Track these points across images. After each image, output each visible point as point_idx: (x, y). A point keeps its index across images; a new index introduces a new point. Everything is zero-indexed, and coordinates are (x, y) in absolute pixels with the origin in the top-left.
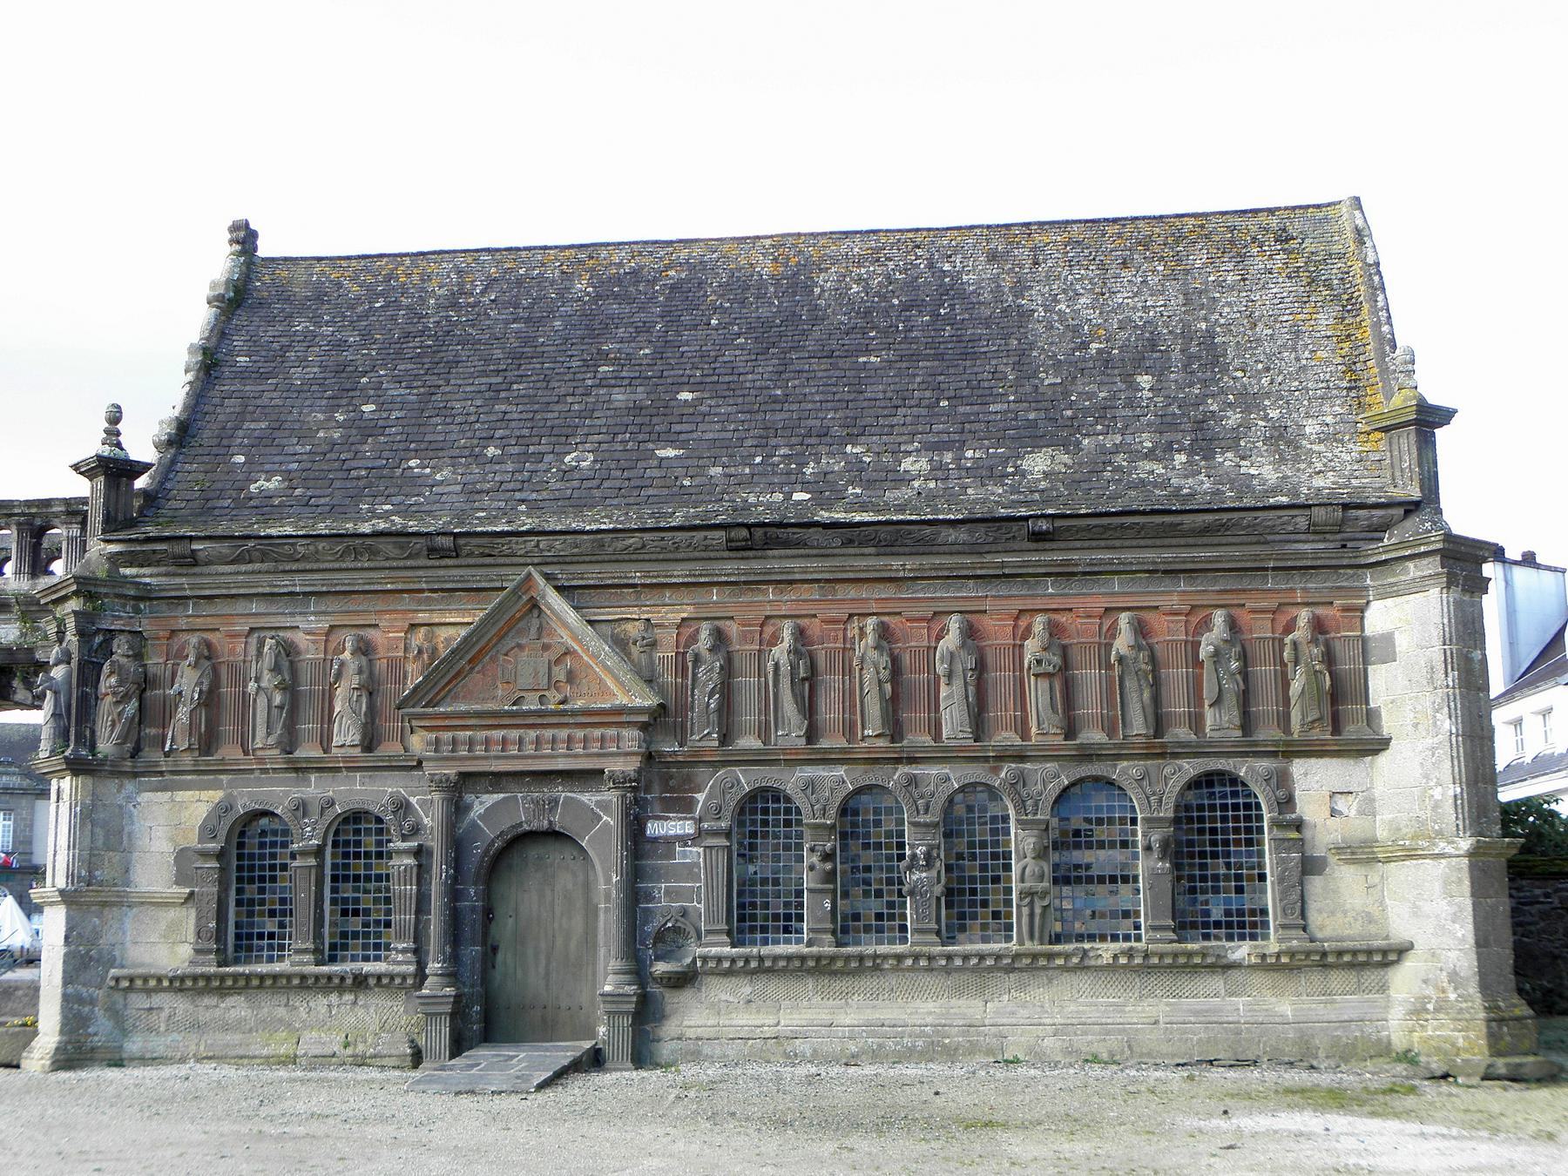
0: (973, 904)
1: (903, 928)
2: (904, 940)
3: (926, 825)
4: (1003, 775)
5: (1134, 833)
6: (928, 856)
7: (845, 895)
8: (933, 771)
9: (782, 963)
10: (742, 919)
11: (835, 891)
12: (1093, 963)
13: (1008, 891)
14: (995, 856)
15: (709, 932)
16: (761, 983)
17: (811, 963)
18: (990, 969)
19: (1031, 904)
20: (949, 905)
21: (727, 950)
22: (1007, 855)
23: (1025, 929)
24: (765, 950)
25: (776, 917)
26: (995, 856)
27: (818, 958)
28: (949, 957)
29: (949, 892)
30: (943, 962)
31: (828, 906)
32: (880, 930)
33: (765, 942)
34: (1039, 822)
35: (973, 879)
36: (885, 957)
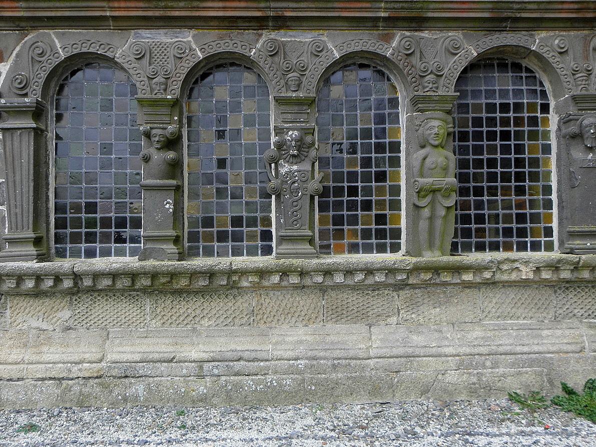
0: (352, 206)
1: (266, 236)
2: (267, 251)
3: (299, 102)
5: (546, 121)
6: (301, 145)
7: (194, 195)
8: (305, 37)
9: (106, 282)
10: (61, 224)
11: (178, 189)
12: (505, 277)
13: (396, 190)
14: (380, 148)
15: (12, 242)
16: (84, 304)
17: (146, 282)
18: (377, 287)
19: (432, 203)
20: (323, 207)
21: (34, 265)
22: (395, 147)
24: (82, 264)
25: (106, 223)
26: (380, 148)
27: (154, 275)
28: (328, 272)
29: (325, 193)
30: (320, 279)
31: (169, 207)
32: (237, 237)
33: (90, 254)
34: (443, 99)
35: (352, 176)
36: (243, 273)
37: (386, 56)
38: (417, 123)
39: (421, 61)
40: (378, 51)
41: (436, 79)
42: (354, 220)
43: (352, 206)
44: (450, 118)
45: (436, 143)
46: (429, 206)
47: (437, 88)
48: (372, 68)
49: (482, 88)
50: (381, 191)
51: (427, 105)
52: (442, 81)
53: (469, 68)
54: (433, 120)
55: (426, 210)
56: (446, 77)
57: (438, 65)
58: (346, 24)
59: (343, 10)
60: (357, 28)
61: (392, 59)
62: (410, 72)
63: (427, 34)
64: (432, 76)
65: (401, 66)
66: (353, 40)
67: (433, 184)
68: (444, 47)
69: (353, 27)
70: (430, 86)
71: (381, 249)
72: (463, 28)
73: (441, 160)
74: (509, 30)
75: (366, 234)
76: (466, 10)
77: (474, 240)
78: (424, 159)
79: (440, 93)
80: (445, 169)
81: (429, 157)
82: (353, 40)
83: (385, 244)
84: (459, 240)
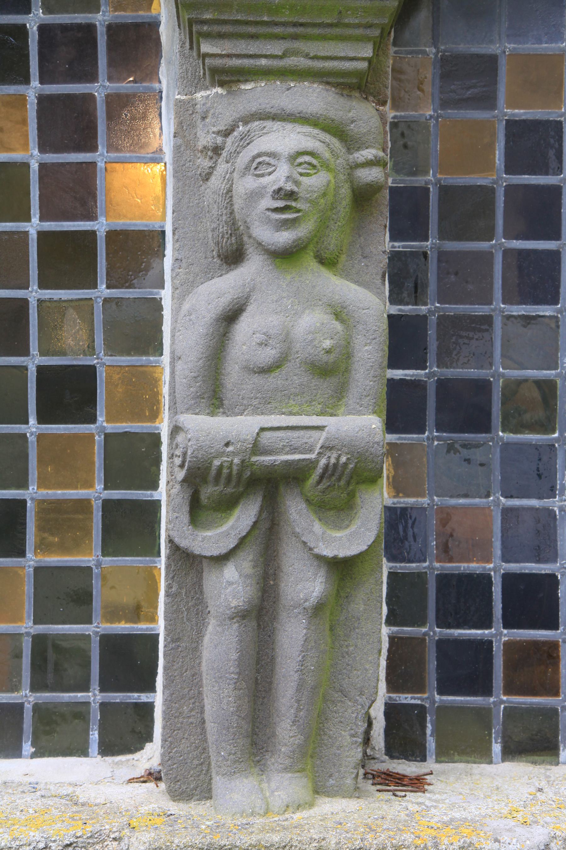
19: (267, 539)
23: (219, 699)
44: (364, 116)
45: (284, 238)
51: (242, 47)
54: (277, 125)
55: (230, 572)
67: (257, 448)
73: (312, 326)
77: (500, 700)
78: (231, 316)
80: (331, 372)
81: (251, 309)
83: (80, 713)
84: (432, 698)
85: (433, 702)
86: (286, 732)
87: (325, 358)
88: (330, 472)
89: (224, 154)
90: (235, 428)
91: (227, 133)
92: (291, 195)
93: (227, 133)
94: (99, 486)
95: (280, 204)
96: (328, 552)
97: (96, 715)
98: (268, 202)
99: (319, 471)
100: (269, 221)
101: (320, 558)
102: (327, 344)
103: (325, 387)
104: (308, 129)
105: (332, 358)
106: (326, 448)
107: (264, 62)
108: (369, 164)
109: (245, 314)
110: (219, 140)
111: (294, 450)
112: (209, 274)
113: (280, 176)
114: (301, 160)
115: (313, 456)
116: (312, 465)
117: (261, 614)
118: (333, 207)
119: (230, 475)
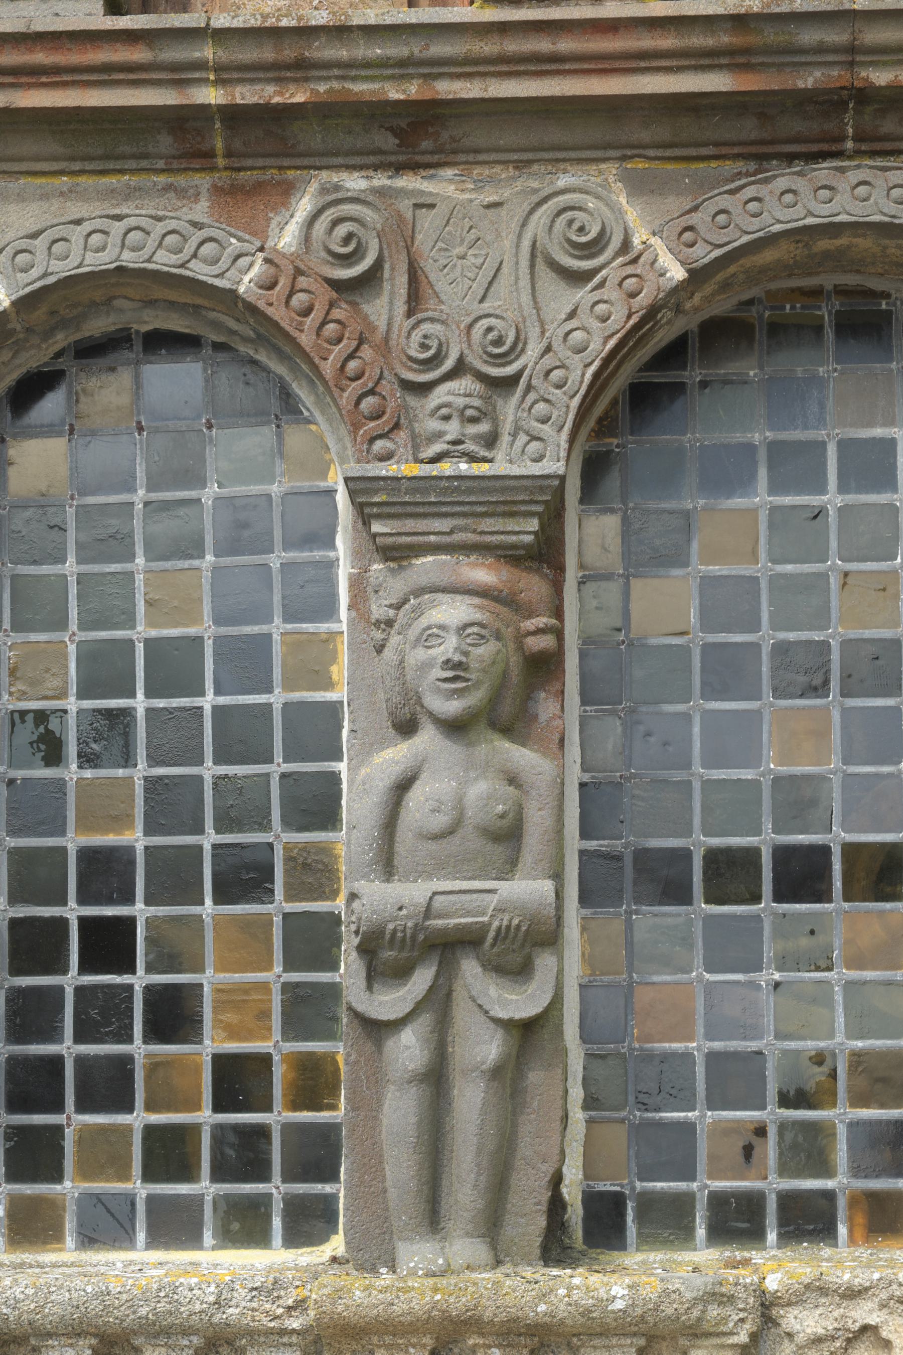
0: (102, 1015)
4: (287, 237)
23: (400, 1168)
26: (241, 736)
34: (503, 497)
37: (233, 293)
38: (378, 610)
39: (410, 313)
40: (200, 271)
41: (486, 399)
42: (108, 1087)
43: (102, 1015)
44: (533, 586)
45: (452, 707)
46: (425, 1020)
47: (491, 441)
48: (207, 351)
49: (757, 437)
50: (248, 943)
51: (410, 525)
52: (509, 409)
53: (694, 345)
56: (529, 388)
57: (490, 329)
58: (52, 147)
59: (23, 80)
60: (107, 162)
61: (261, 305)
62: (353, 365)
63: (450, 181)
64: (465, 383)
65: (306, 340)
66: (78, 222)
67: (428, 912)
68: (526, 244)
69: (91, 159)
70: (453, 429)
71: (245, 1225)
72: (627, 151)
73: (482, 794)
74: (858, 153)
75: (169, 1153)
76: (618, 64)
79: (501, 467)
81: (424, 776)
82: (78, 222)
85: (633, 1189)
86: (465, 1191)
87: (499, 823)
88: (503, 935)
89: (396, 626)
90: (411, 892)
91: (398, 607)
92: (459, 665)
93: (398, 607)
94: (278, 969)
95: (450, 674)
96: (503, 1015)
97: (278, 1207)
98: (438, 673)
99: (492, 934)
100: (439, 690)
101: (497, 1021)
102: (500, 808)
103: (499, 852)
104: (477, 601)
105: (505, 822)
106: (499, 910)
107: (432, 538)
108: (539, 631)
109: (418, 782)
110: (391, 613)
111: (468, 913)
112: (383, 745)
113: (448, 647)
114: (469, 631)
115: (486, 919)
116: (484, 928)
117: (436, 1078)
118: (505, 674)
119: (404, 939)
